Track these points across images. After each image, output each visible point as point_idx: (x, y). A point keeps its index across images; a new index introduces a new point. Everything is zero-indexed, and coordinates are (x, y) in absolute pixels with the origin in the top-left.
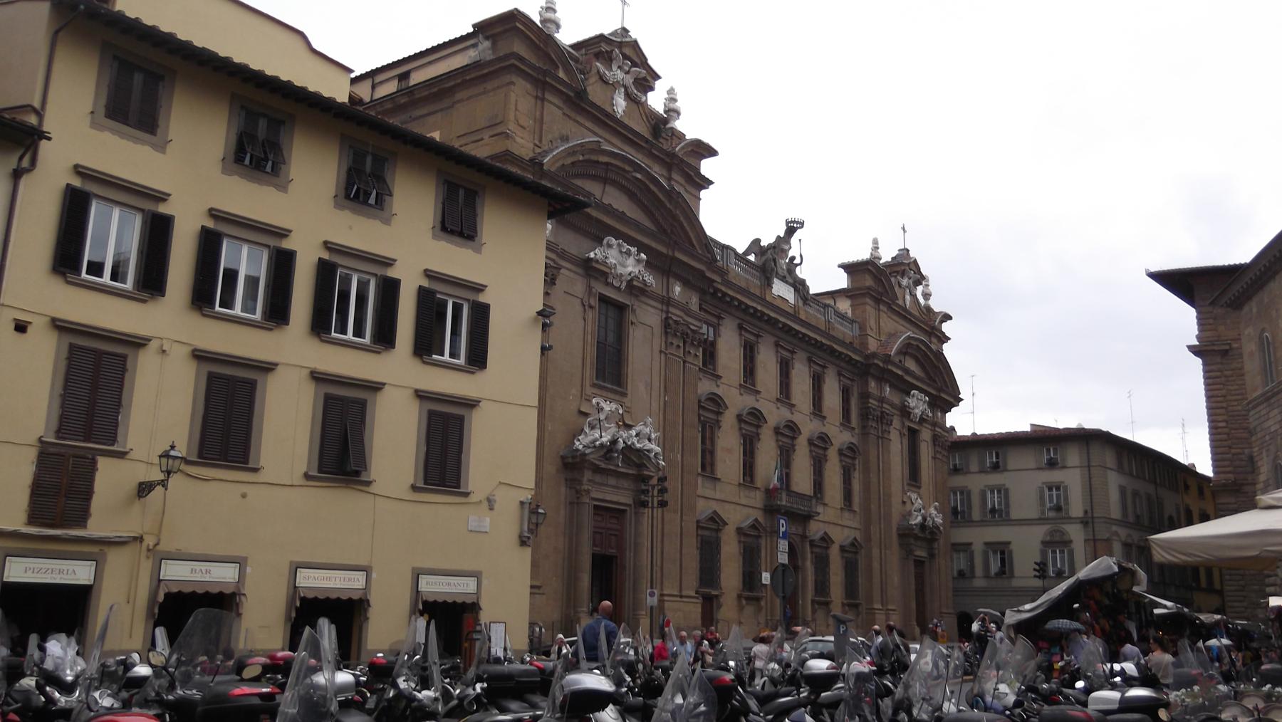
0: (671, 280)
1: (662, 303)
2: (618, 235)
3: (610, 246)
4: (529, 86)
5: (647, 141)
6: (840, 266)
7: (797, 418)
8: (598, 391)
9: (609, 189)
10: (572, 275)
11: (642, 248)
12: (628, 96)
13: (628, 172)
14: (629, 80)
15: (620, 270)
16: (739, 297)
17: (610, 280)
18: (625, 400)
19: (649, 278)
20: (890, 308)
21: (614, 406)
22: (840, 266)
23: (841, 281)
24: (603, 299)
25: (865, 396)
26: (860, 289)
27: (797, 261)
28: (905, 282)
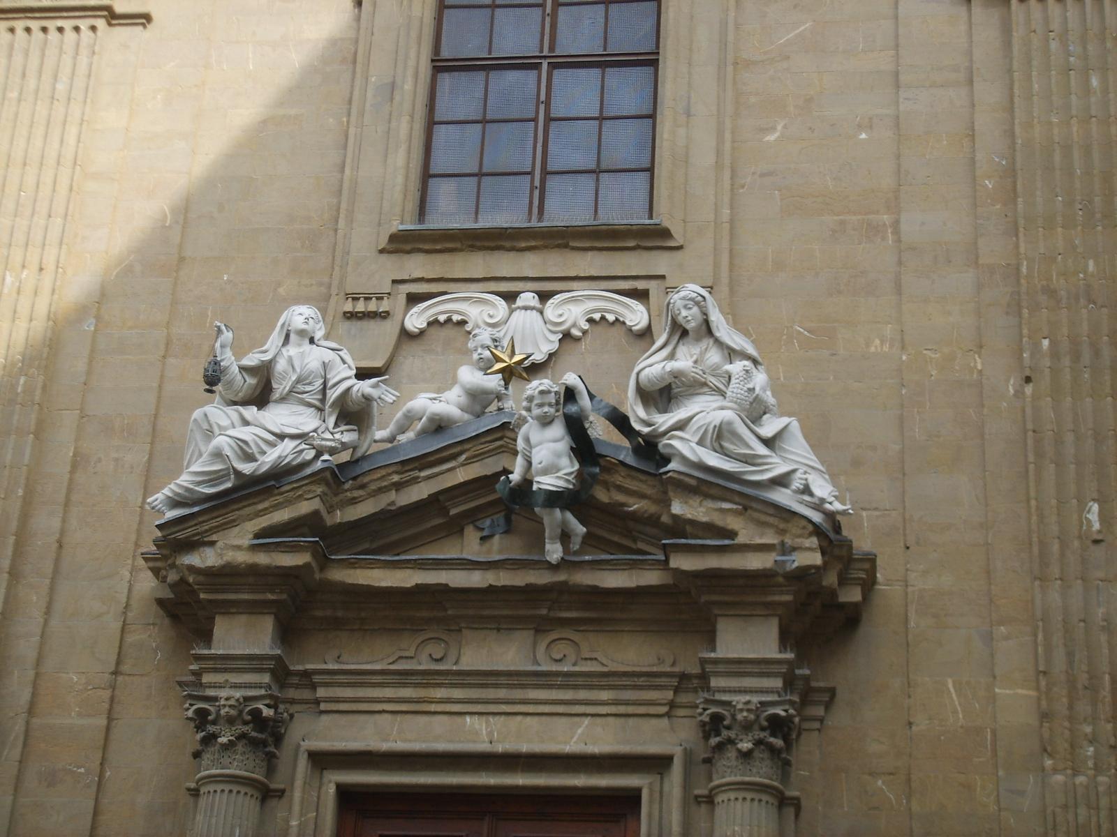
8: (417, 266)
21: (571, 310)
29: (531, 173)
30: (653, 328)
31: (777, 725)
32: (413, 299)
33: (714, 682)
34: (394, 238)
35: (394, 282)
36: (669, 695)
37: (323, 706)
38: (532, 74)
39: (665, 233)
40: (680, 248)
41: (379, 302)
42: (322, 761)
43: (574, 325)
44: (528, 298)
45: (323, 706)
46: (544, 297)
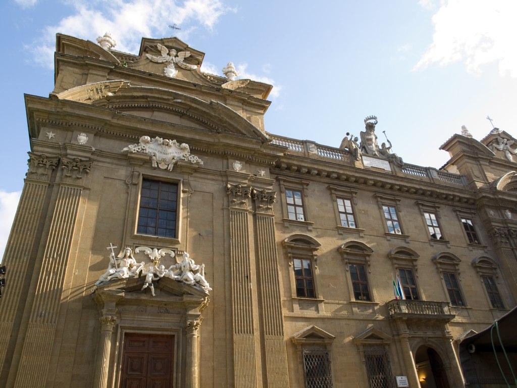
0: (230, 161)
1: (221, 176)
2: (153, 135)
3: (146, 142)
4: (76, 70)
5: (195, 85)
6: (440, 149)
7: (412, 246)
9: (156, 113)
10: (114, 166)
11: (180, 140)
12: (177, 67)
13: (168, 100)
14: (180, 59)
15: (159, 156)
16: (316, 167)
17: (155, 165)
18: (176, 246)
19: (195, 159)
20: (490, 162)
21: (163, 252)
22: (440, 149)
23: (446, 156)
24: (146, 179)
25: (487, 222)
26: (457, 155)
27: (387, 145)
28: (501, 147)
32: (136, 247)
42: (122, 328)
46: (158, 250)
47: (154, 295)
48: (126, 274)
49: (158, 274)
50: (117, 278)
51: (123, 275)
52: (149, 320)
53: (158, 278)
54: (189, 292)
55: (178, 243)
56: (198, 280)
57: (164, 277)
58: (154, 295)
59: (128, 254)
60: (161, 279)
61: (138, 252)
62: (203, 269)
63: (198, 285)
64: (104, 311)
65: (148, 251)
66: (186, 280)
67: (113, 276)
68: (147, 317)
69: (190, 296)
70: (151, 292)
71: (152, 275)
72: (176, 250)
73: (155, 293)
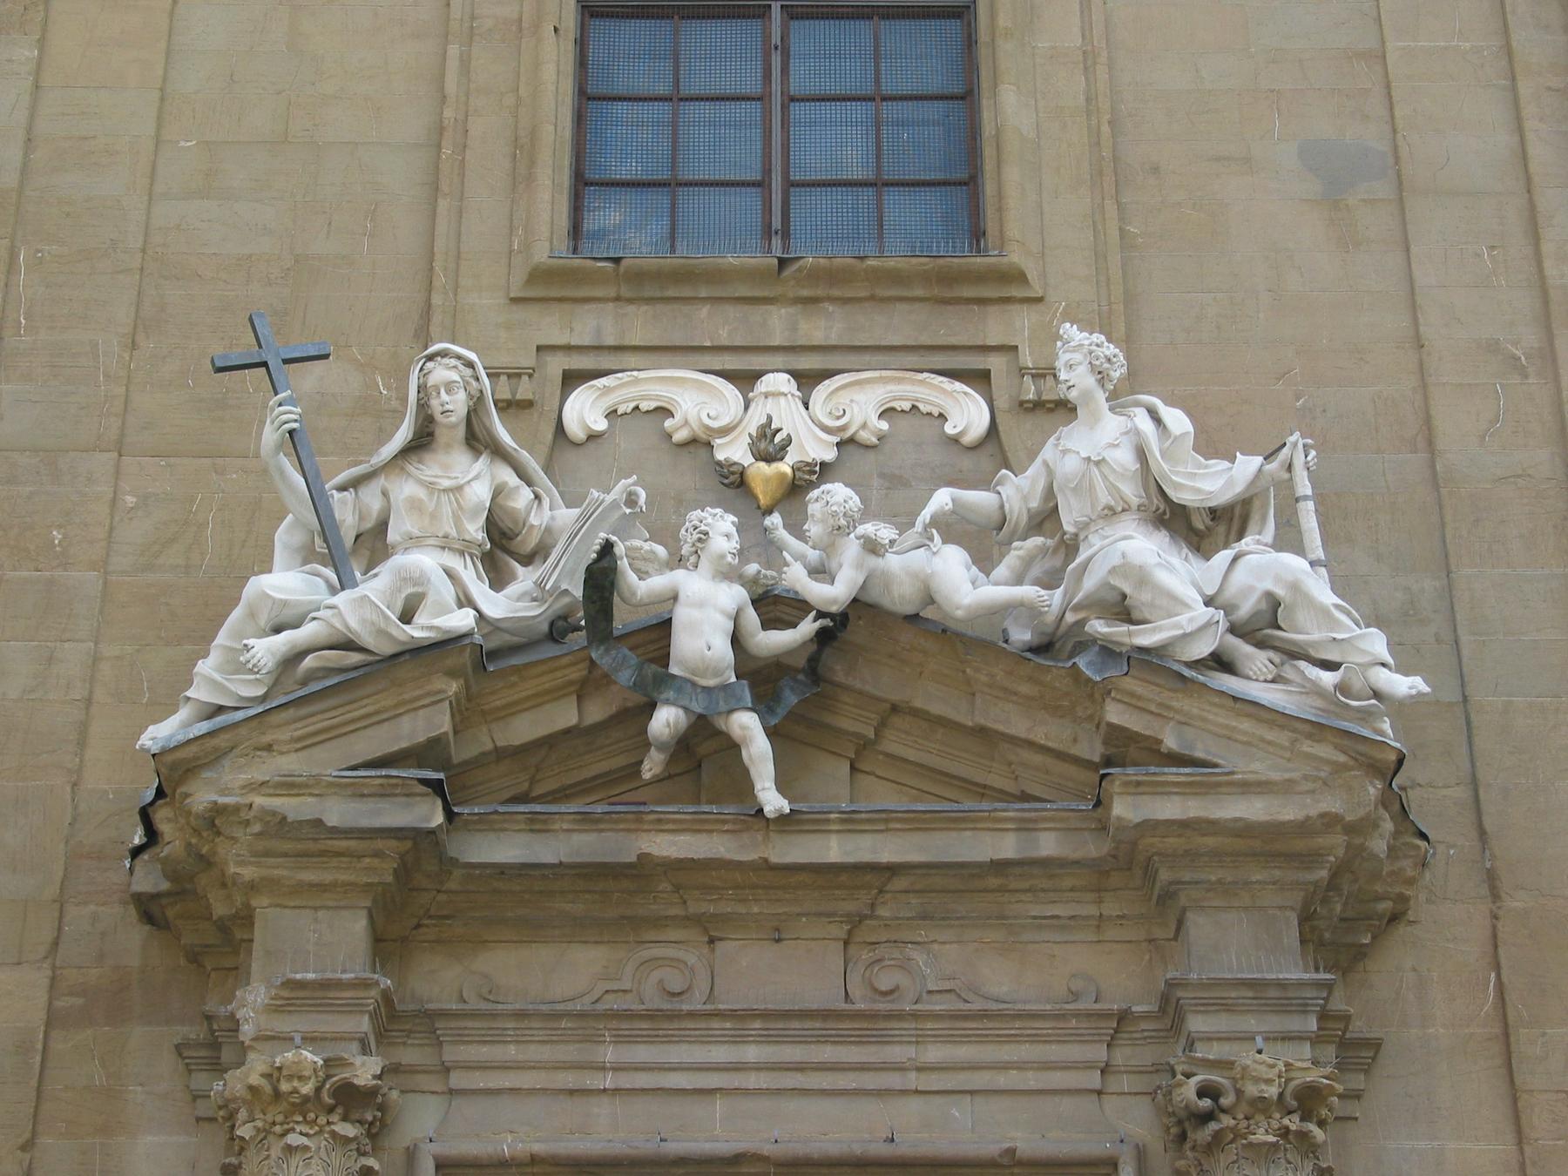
21: (859, 401)
29: (762, 184)
30: (1001, 428)
31: (1308, 1101)
32: (572, 379)
33: (1197, 1023)
34: (539, 275)
35: (539, 348)
36: (1099, 1053)
37: (457, 1080)
38: (755, 26)
39: (1020, 277)
40: (1040, 300)
41: (514, 381)
43: (864, 426)
44: (779, 381)
45: (457, 1080)
46: (807, 381)
47: (773, 801)
48: (437, 587)
49: (796, 577)
50: (349, 645)
51: (407, 617)
52: (752, 1080)
53: (808, 627)
54: (1171, 742)
55: (1008, 286)
56: (1245, 610)
57: (860, 607)
58: (773, 801)
59: (455, 404)
60: (837, 628)
61: (601, 425)
62: (1304, 487)
63: (1257, 661)
64: (252, 1004)
65: (699, 401)
66: (1122, 610)
67: (308, 632)
68: (720, 1054)
69: (1173, 774)
70: (742, 784)
71: (733, 596)
72: (995, 363)
73: (782, 786)
